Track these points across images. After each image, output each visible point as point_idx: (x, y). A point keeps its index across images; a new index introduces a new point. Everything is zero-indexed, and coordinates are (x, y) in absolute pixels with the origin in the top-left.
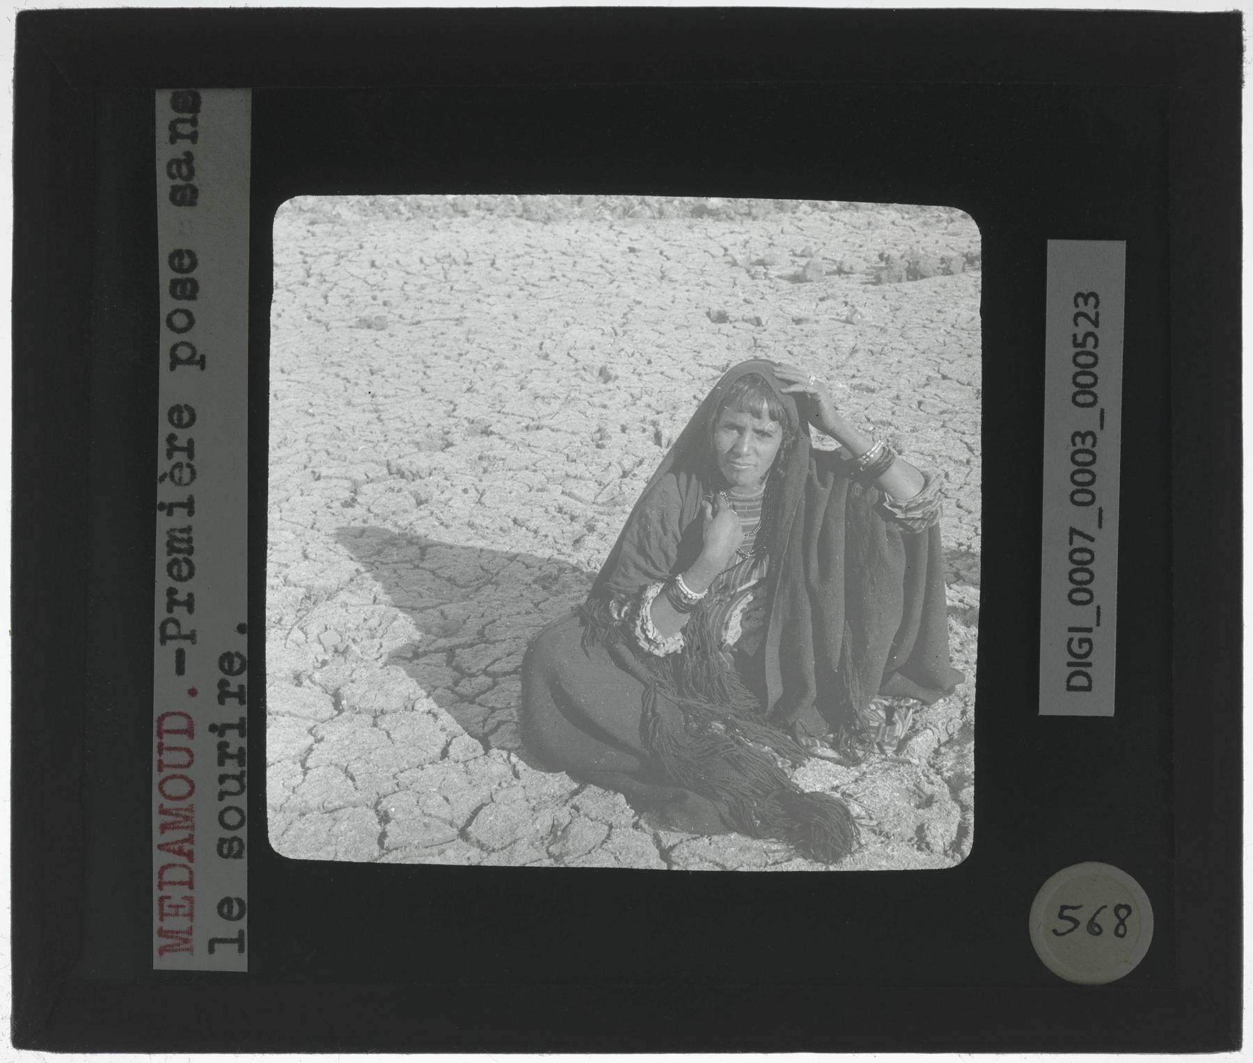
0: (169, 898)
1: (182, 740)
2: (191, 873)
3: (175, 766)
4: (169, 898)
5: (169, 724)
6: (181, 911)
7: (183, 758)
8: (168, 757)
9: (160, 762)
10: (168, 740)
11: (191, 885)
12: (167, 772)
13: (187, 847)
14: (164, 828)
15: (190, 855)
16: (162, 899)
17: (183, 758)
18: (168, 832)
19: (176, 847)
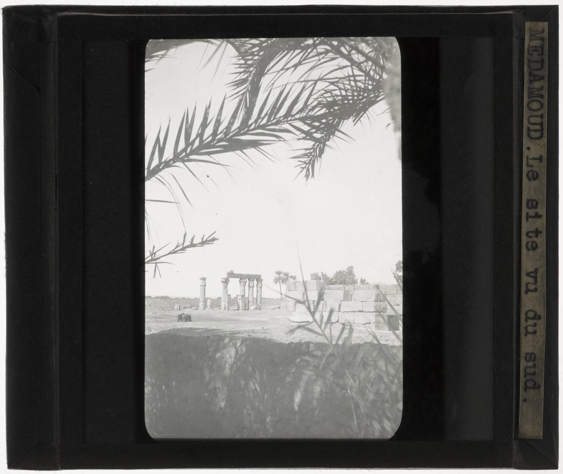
0: (539, 55)
1: (532, 127)
2: (529, 66)
3: (536, 116)
4: (539, 55)
5: (538, 134)
6: (534, 49)
7: (533, 120)
8: (538, 120)
9: (542, 118)
10: (538, 127)
11: (529, 61)
12: (539, 113)
13: (532, 79)
14: (542, 88)
15: (530, 74)
16: (542, 54)
17: (533, 120)
18: (540, 87)
19: (536, 78)
